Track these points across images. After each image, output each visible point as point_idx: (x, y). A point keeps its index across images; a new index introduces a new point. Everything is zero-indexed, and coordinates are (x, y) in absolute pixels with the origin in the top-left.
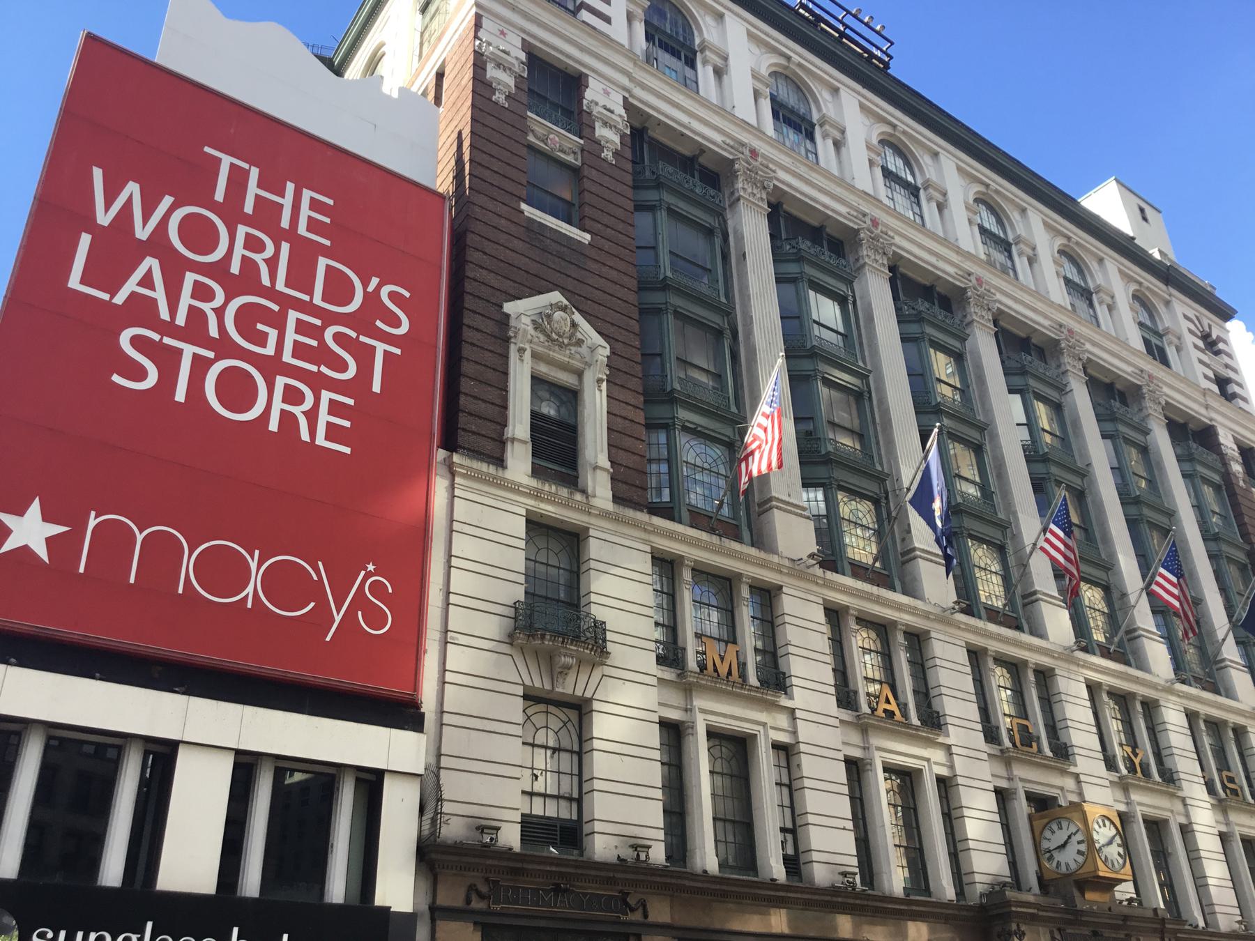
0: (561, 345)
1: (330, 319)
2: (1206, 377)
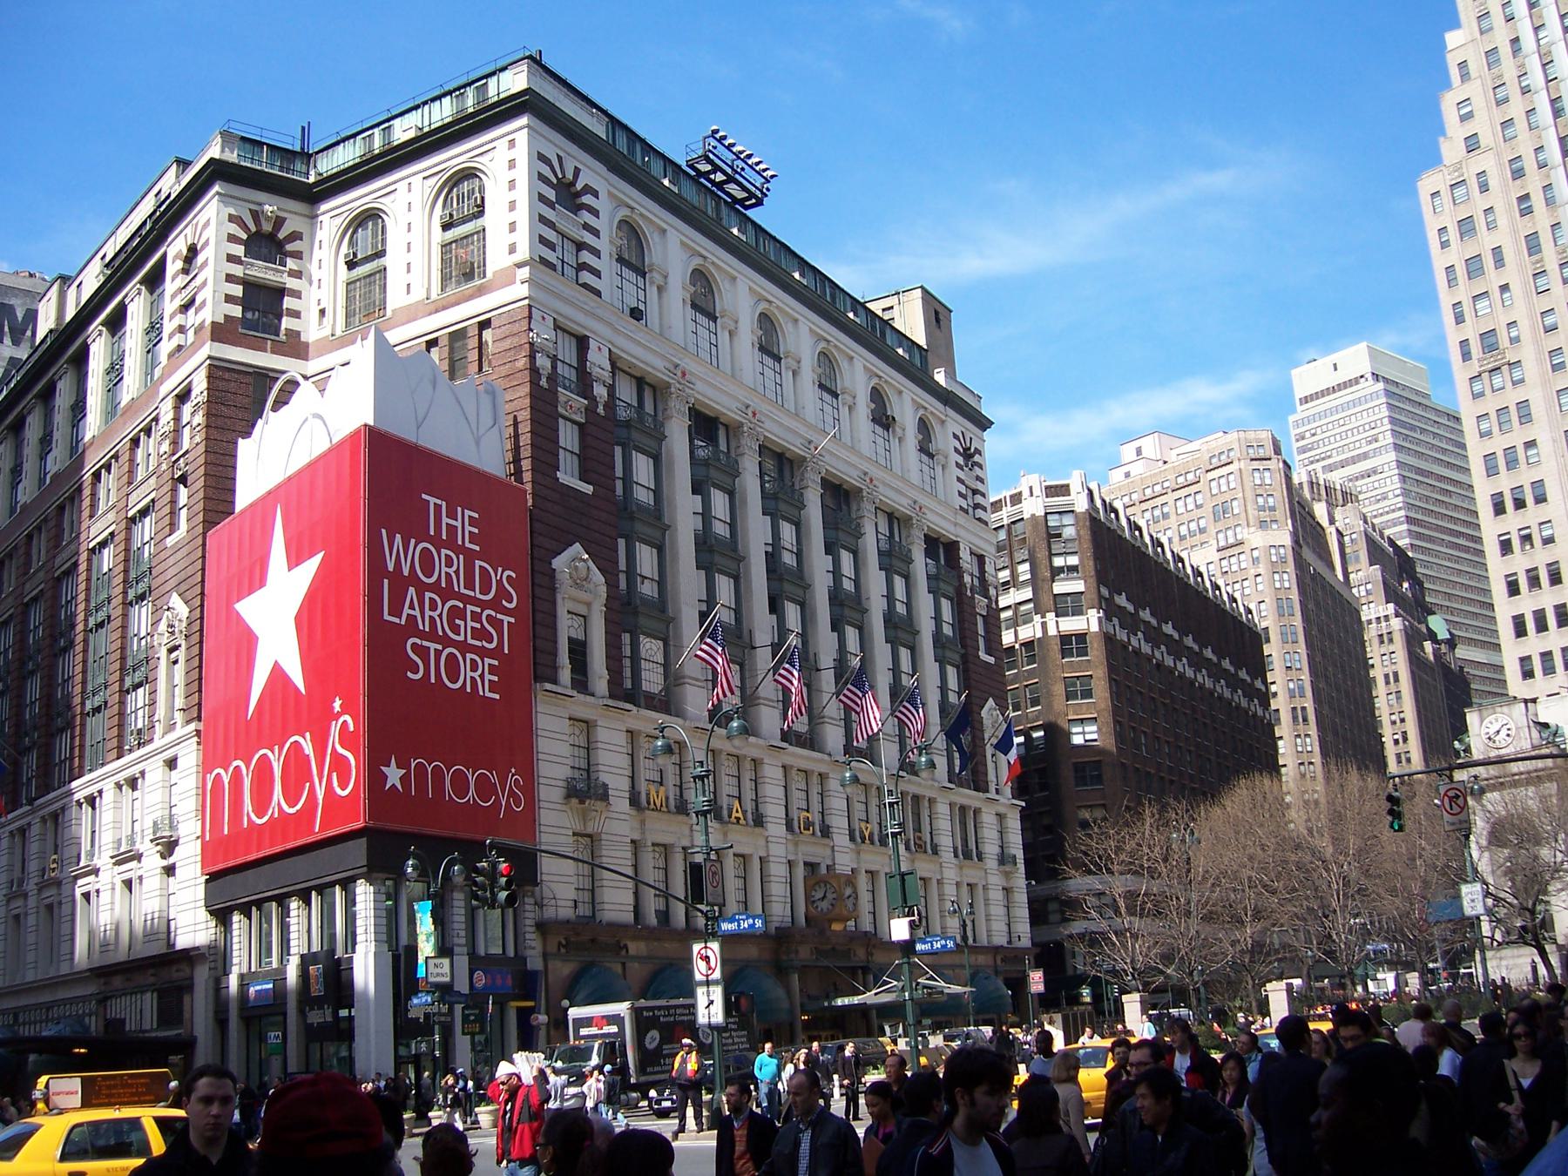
1: (484, 605)
2: (960, 494)
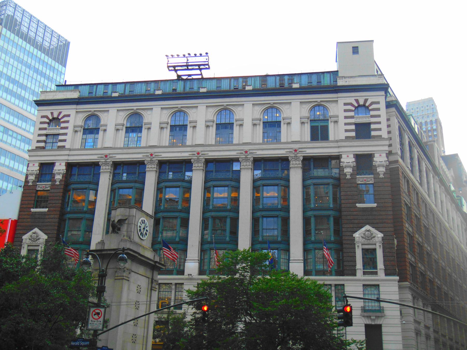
0: (369, 239)
